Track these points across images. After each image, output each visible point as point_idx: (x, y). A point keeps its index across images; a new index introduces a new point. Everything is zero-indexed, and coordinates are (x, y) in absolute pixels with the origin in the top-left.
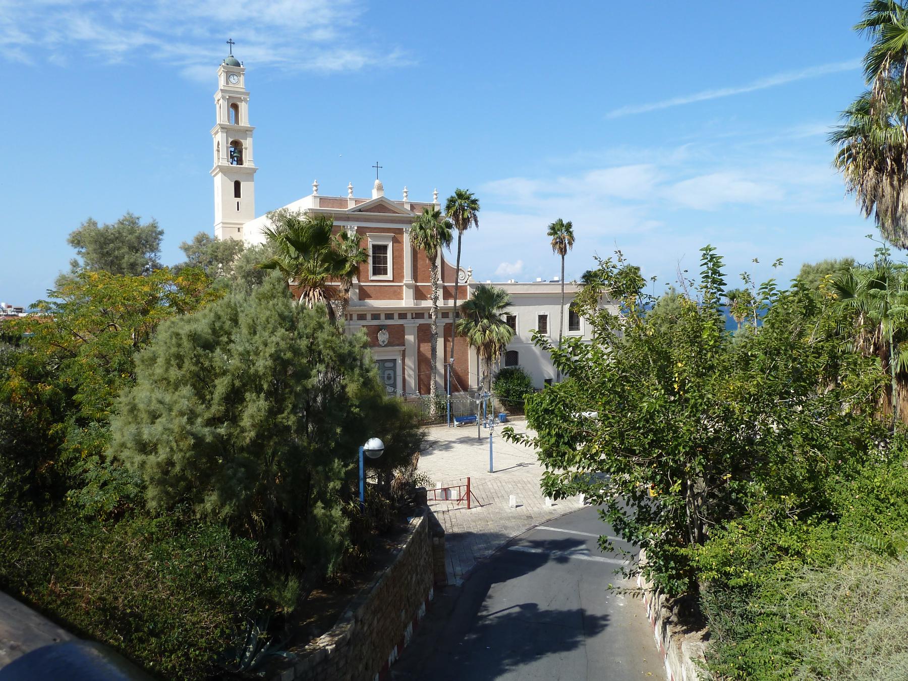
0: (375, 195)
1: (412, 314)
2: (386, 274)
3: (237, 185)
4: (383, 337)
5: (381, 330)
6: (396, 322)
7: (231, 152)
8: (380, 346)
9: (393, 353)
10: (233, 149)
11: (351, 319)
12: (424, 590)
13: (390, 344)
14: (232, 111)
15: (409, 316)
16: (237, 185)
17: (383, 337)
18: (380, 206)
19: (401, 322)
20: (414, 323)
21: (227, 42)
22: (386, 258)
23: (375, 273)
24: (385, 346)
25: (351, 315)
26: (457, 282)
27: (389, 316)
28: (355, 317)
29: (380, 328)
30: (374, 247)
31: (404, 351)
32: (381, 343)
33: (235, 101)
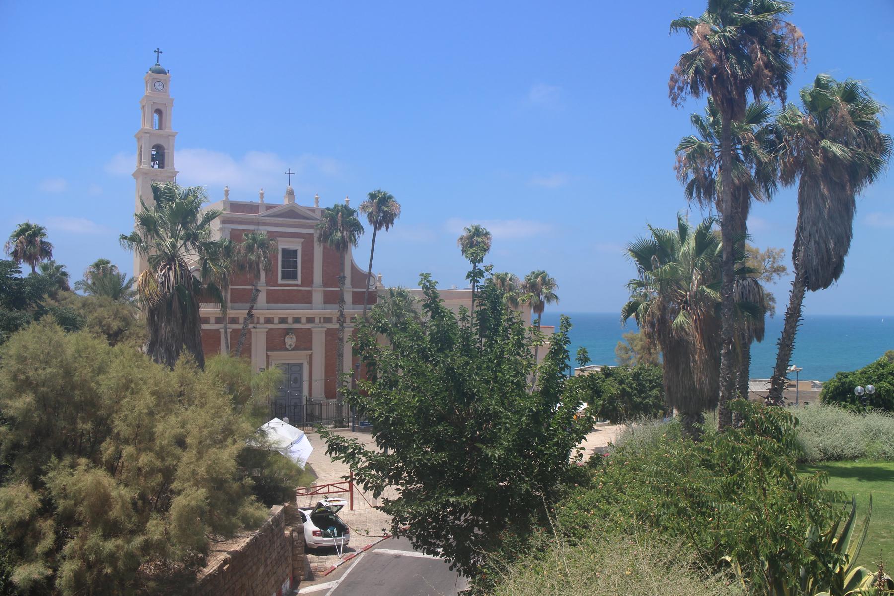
0: (285, 202)
1: (320, 318)
2: (294, 277)
5: (287, 334)
7: (153, 155)
8: (287, 350)
9: (300, 357)
10: (155, 153)
11: (258, 322)
12: (276, 582)
13: (296, 348)
14: (156, 117)
17: (290, 341)
18: (292, 213)
20: (322, 327)
21: (155, 51)
22: (295, 262)
24: (292, 350)
25: (258, 318)
26: (368, 288)
27: (297, 320)
28: (262, 320)
29: (287, 332)
30: (284, 251)
31: (311, 355)
32: (287, 347)
33: (160, 107)
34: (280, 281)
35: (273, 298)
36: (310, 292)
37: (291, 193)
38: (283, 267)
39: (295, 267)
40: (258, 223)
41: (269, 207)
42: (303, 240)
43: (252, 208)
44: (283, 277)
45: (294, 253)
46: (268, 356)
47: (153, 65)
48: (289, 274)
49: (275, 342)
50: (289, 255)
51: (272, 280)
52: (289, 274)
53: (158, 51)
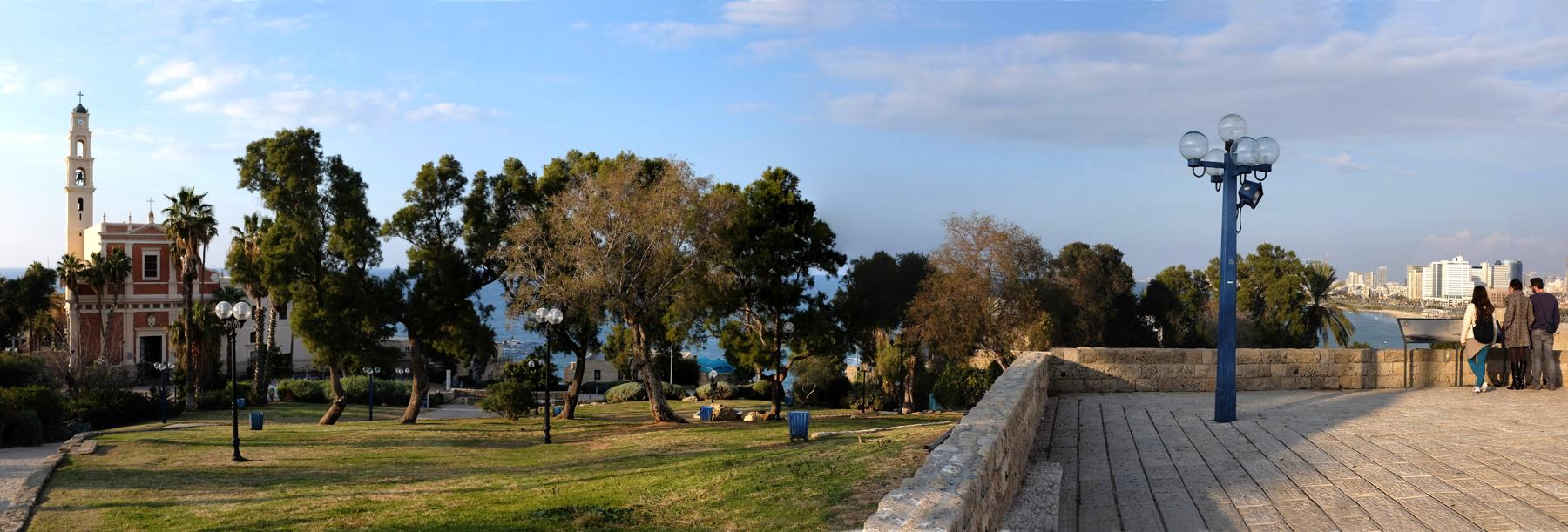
2: (155, 275)
3: (80, 201)
4: (152, 320)
6: (162, 309)
11: (128, 307)
13: (157, 325)
15: (172, 306)
16: (80, 201)
17: (152, 320)
19: (166, 310)
22: (155, 265)
23: (147, 275)
24: (154, 326)
27: (157, 306)
28: (130, 306)
29: (150, 314)
30: (147, 257)
34: (144, 278)
35: (138, 290)
36: (167, 286)
37: (151, 215)
38: (146, 268)
39: (155, 268)
40: (127, 238)
41: (135, 226)
42: (160, 249)
43: (123, 227)
44: (147, 275)
45: (155, 257)
46: (135, 332)
47: (77, 105)
48: (151, 272)
49: (140, 321)
50: (151, 260)
51: (137, 277)
52: (151, 272)
53: (80, 95)
